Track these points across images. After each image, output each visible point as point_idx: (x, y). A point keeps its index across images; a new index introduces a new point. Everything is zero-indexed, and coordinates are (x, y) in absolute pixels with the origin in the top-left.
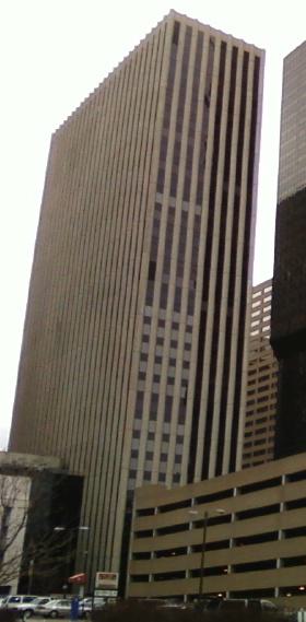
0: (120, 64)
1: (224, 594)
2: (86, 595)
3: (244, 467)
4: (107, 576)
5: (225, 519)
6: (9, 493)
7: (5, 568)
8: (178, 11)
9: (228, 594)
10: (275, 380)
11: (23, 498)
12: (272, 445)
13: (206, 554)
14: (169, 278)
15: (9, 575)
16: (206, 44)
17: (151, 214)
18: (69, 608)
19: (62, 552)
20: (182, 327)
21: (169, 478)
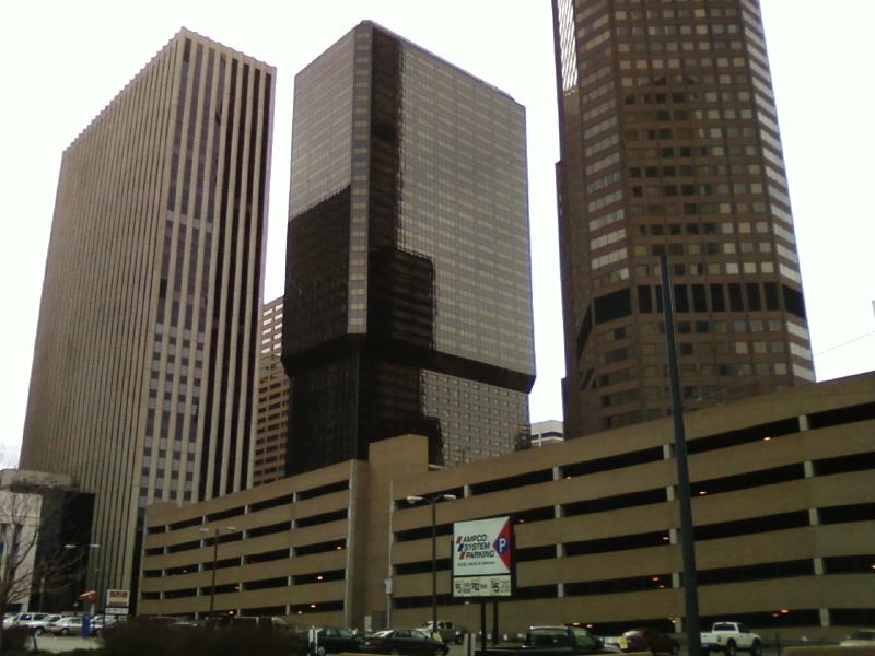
0: (131, 81)
1: (235, 612)
2: (97, 613)
3: (256, 484)
4: (118, 594)
5: (236, 537)
6: (20, 510)
7: (16, 585)
8: (189, 29)
9: (239, 612)
10: (287, 397)
11: (34, 515)
12: (283, 462)
13: (216, 597)
14: (180, 297)
15: (20, 593)
16: (217, 61)
17: (162, 232)
18: (80, 625)
19: (74, 569)
20: (193, 345)
21: (180, 496)
